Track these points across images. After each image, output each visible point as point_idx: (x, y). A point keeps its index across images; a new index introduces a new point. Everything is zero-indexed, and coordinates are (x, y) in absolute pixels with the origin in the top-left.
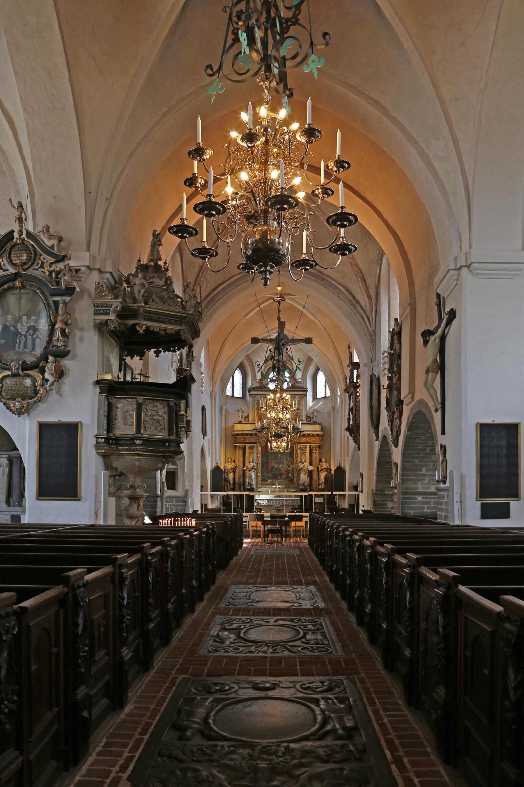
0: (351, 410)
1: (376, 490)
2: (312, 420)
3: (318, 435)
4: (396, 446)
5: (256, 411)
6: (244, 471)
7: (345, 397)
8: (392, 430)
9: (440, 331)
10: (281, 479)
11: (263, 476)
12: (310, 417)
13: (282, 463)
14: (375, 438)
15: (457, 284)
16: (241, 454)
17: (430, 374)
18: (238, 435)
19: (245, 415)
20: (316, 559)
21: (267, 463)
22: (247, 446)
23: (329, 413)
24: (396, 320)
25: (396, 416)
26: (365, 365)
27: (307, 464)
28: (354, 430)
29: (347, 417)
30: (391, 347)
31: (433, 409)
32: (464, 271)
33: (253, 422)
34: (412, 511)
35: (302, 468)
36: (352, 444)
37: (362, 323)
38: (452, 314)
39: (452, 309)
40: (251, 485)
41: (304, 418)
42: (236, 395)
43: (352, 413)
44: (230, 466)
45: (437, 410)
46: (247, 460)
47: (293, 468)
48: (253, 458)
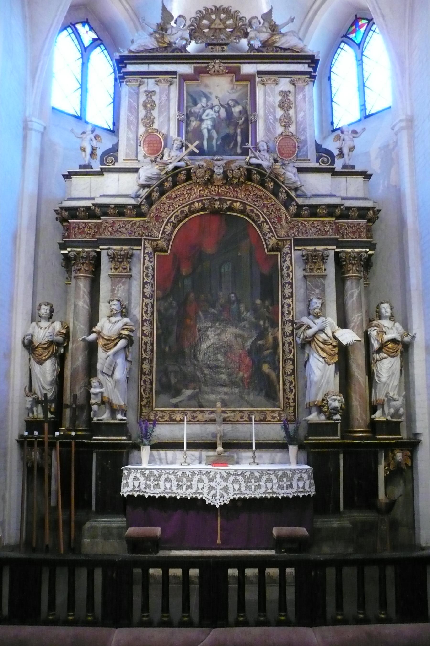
3: (362, 213)
6: (92, 349)
11: (163, 372)
16: (83, 286)
18: (73, 212)
27: (331, 320)
33: (128, 165)
35: (314, 336)
41: (312, 153)
46: (104, 308)
47: (276, 339)
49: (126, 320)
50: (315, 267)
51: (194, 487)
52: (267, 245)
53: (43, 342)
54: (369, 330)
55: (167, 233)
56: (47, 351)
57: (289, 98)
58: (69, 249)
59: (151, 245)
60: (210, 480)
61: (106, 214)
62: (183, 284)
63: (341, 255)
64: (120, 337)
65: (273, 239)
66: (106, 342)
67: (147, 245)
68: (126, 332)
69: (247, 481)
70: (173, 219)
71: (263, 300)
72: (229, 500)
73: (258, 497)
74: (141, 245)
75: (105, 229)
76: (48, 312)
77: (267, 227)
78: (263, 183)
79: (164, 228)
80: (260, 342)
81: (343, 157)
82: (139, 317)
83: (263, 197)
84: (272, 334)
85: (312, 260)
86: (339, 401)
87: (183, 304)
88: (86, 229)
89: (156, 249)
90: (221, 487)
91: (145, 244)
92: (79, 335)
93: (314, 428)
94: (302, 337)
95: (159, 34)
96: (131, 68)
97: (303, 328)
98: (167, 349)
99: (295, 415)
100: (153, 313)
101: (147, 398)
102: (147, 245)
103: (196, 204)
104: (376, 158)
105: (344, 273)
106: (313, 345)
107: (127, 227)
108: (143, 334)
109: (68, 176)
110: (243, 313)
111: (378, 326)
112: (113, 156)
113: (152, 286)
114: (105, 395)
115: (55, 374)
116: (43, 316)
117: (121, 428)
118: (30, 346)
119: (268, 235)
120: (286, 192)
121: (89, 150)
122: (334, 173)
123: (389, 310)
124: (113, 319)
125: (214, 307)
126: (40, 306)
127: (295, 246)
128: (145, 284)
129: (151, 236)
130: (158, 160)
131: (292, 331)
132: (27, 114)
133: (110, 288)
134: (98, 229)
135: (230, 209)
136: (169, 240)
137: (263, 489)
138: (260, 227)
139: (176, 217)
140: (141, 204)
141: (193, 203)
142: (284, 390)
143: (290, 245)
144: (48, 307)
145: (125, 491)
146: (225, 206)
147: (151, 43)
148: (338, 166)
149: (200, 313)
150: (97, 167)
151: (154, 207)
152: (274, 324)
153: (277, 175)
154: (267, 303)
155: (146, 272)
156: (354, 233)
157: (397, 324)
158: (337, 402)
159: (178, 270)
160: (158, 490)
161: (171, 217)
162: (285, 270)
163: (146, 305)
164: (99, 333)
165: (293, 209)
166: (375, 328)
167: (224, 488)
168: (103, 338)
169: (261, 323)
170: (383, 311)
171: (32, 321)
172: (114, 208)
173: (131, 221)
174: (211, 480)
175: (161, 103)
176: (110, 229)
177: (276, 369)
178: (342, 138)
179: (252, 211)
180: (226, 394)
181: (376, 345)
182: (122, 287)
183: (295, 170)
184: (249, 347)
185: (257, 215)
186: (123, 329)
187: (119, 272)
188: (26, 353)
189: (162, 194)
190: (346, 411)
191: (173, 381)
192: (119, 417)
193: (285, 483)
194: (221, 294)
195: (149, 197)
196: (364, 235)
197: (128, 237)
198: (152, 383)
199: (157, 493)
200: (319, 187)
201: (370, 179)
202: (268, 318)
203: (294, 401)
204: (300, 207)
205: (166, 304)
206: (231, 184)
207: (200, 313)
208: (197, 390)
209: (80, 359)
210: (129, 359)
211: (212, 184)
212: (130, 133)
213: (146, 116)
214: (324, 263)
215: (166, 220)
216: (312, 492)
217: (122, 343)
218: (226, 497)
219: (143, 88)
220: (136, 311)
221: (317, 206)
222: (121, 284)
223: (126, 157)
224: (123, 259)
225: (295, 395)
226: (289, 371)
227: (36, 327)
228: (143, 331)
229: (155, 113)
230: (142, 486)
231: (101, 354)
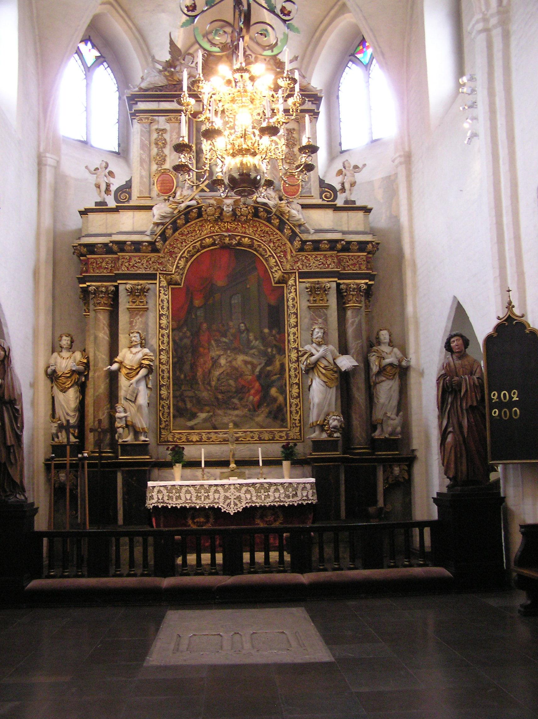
3: (362, 246)
5: (154, 167)
6: (113, 377)
10: (244, 407)
11: (179, 398)
13: (245, 348)
16: (103, 319)
18: (91, 248)
19: (116, 184)
21: (195, 350)
22: (125, 286)
46: (123, 339)
47: (282, 365)
48: (146, 329)
49: (146, 350)
50: (318, 298)
51: (211, 497)
52: (274, 278)
53: (66, 372)
54: (369, 355)
55: (180, 268)
56: (70, 380)
57: (294, 135)
58: (88, 284)
59: (166, 279)
61: (122, 250)
62: (196, 315)
63: (342, 286)
64: (141, 366)
65: (280, 272)
66: (128, 371)
67: (162, 279)
68: (147, 362)
69: (257, 491)
70: (185, 254)
71: (271, 328)
72: (242, 508)
73: (267, 505)
74: (156, 279)
75: (122, 265)
76: (69, 342)
77: (274, 260)
78: (269, 220)
79: (178, 263)
80: (269, 368)
81: (345, 192)
82: (156, 347)
83: (270, 233)
84: (279, 361)
85: (315, 291)
86: (338, 420)
87: (196, 334)
88: (104, 264)
89: (169, 283)
90: (235, 497)
91: (160, 278)
92: (101, 365)
93: (318, 445)
94: (305, 363)
95: (169, 72)
96: (142, 106)
97: (306, 356)
98: (182, 376)
99: (300, 435)
100: (168, 343)
101: (165, 422)
102: (162, 279)
103: (207, 240)
104: (380, 188)
105: (344, 303)
106: (315, 371)
107: (142, 262)
108: (160, 363)
109: (84, 213)
110: (252, 342)
111: (377, 351)
112: (125, 192)
113: (168, 317)
114: (129, 419)
115: (78, 401)
116: (65, 346)
117: (143, 448)
118: (53, 376)
119: (275, 269)
120: (291, 228)
121: (103, 187)
122: (336, 209)
123: (387, 337)
124: (134, 350)
125: (226, 337)
126: (61, 337)
127: (299, 278)
128: (161, 315)
129: (165, 271)
130: (171, 199)
131: (298, 358)
132: (42, 150)
133: (128, 320)
134: (115, 263)
135: (239, 244)
136: (182, 274)
137: (272, 498)
138: (267, 260)
139: (189, 252)
140: (155, 241)
141: (204, 239)
142: (291, 412)
143: (295, 277)
144: (69, 338)
145: (151, 503)
146: (234, 242)
147: (160, 80)
148: (340, 202)
149: (213, 342)
150: (112, 203)
151: (167, 242)
152: (281, 351)
153: (282, 213)
154: (274, 332)
155: (162, 304)
156: (354, 265)
157: (396, 350)
158: (336, 421)
159: (192, 302)
160: (179, 501)
161: (184, 252)
162: (291, 301)
163: (163, 336)
164: (121, 363)
165: (297, 244)
166: (374, 354)
167: (238, 497)
168: (125, 367)
169: (269, 350)
170: (382, 337)
171: (53, 352)
172: (130, 245)
173: (147, 256)
174: (226, 491)
175: (171, 141)
176: (127, 264)
178: (344, 173)
179: (259, 246)
180: (237, 416)
182: (140, 319)
183: (299, 207)
184: (258, 373)
185: (264, 249)
186: (144, 359)
187: (137, 305)
188: (49, 382)
189: (175, 229)
190: (346, 429)
191: (189, 405)
192: (143, 438)
193: (290, 491)
194: (231, 324)
196: (363, 267)
197: (144, 272)
198: (169, 408)
199: (178, 503)
200: (321, 223)
201: (370, 212)
202: (276, 346)
203: (300, 422)
204: (304, 242)
205: (181, 334)
206: (239, 221)
207: (213, 342)
208: (211, 414)
209: (103, 387)
210: (150, 386)
211: (222, 221)
212: (143, 171)
213: (157, 155)
214: (326, 294)
215: (180, 255)
216: (313, 499)
217: (143, 372)
218: (239, 505)
219: (154, 127)
220: (154, 342)
221: (320, 241)
222: (138, 317)
223: (140, 194)
224: (140, 293)
225: (300, 416)
226: (295, 394)
227: (59, 357)
228: (160, 359)
230: (166, 498)
231: (123, 382)
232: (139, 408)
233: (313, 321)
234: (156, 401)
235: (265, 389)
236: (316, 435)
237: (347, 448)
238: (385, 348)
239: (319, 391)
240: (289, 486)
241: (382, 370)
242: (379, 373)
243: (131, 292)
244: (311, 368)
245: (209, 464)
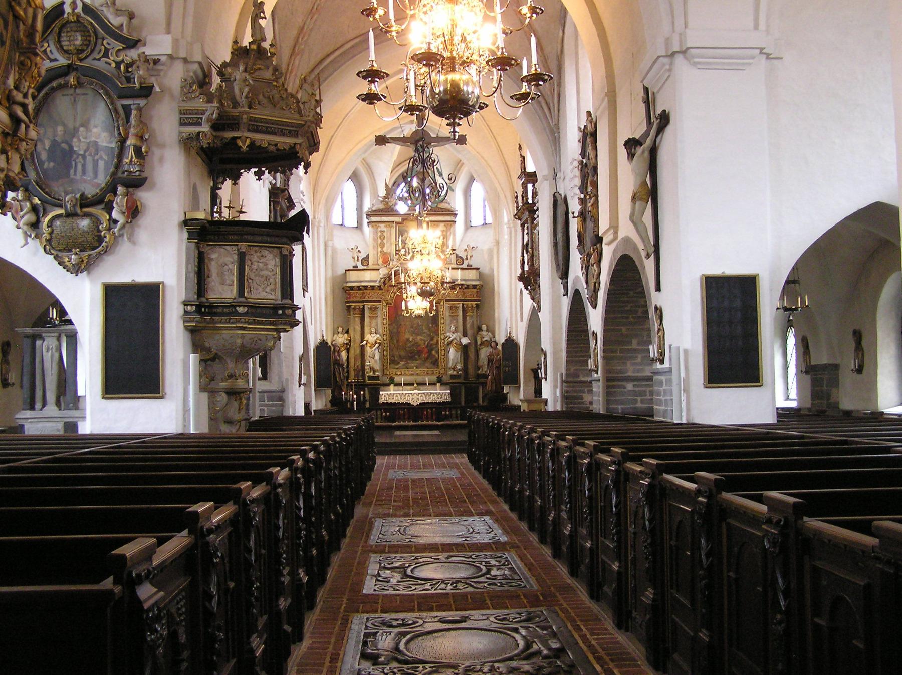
0: (525, 247)
1: (567, 375)
2: (466, 263)
3: (474, 286)
4: (595, 307)
5: (379, 249)
6: (363, 347)
7: (515, 227)
8: (587, 282)
9: (649, 142)
11: (392, 356)
12: (461, 258)
14: (562, 291)
15: (669, 76)
16: (358, 320)
17: (638, 203)
18: (352, 288)
20: (485, 482)
21: (398, 333)
22: (367, 306)
23: (490, 251)
24: (589, 114)
25: (592, 260)
26: (545, 178)
28: (530, 279)
29: (519, 258)
30: (583, 154)
31: (643, 254)
32: (679, 59)
33: (375, 267)
34: (620, 407)
36: (528, 302)
37: (540, 112)
38: (665, 119)
39: (664, 111)
40: (374, 372)
42: (346, 224)
43: (527, 252)
44: (341, 339)
45: (648, 256)
46: (367, 329)
48: (377, 325)
60: (414, 396)
93: (452, 377)
117: (377, 378)
145: (381, 401)
147: (381, 207)
148: (464, 266)
150: (360, 267)
177: (438, 352)
181: (479, 343)
190: (465, 369)
195: (384, 282)
216: (449, 400)
220: (380, 331)
229: (385, 241)
232: (376, 361)
233: (451, 322)
234: (383, 357)
235: (430, 352)
236: (451, 372)
237: (466, 378)
238: (484, 333)
239: (453, 354)
240: (439, 394)
241: (482, 343)
242: (481, 344)
243: (371, 309)
244: (450, 343)
245: (405, 385)
